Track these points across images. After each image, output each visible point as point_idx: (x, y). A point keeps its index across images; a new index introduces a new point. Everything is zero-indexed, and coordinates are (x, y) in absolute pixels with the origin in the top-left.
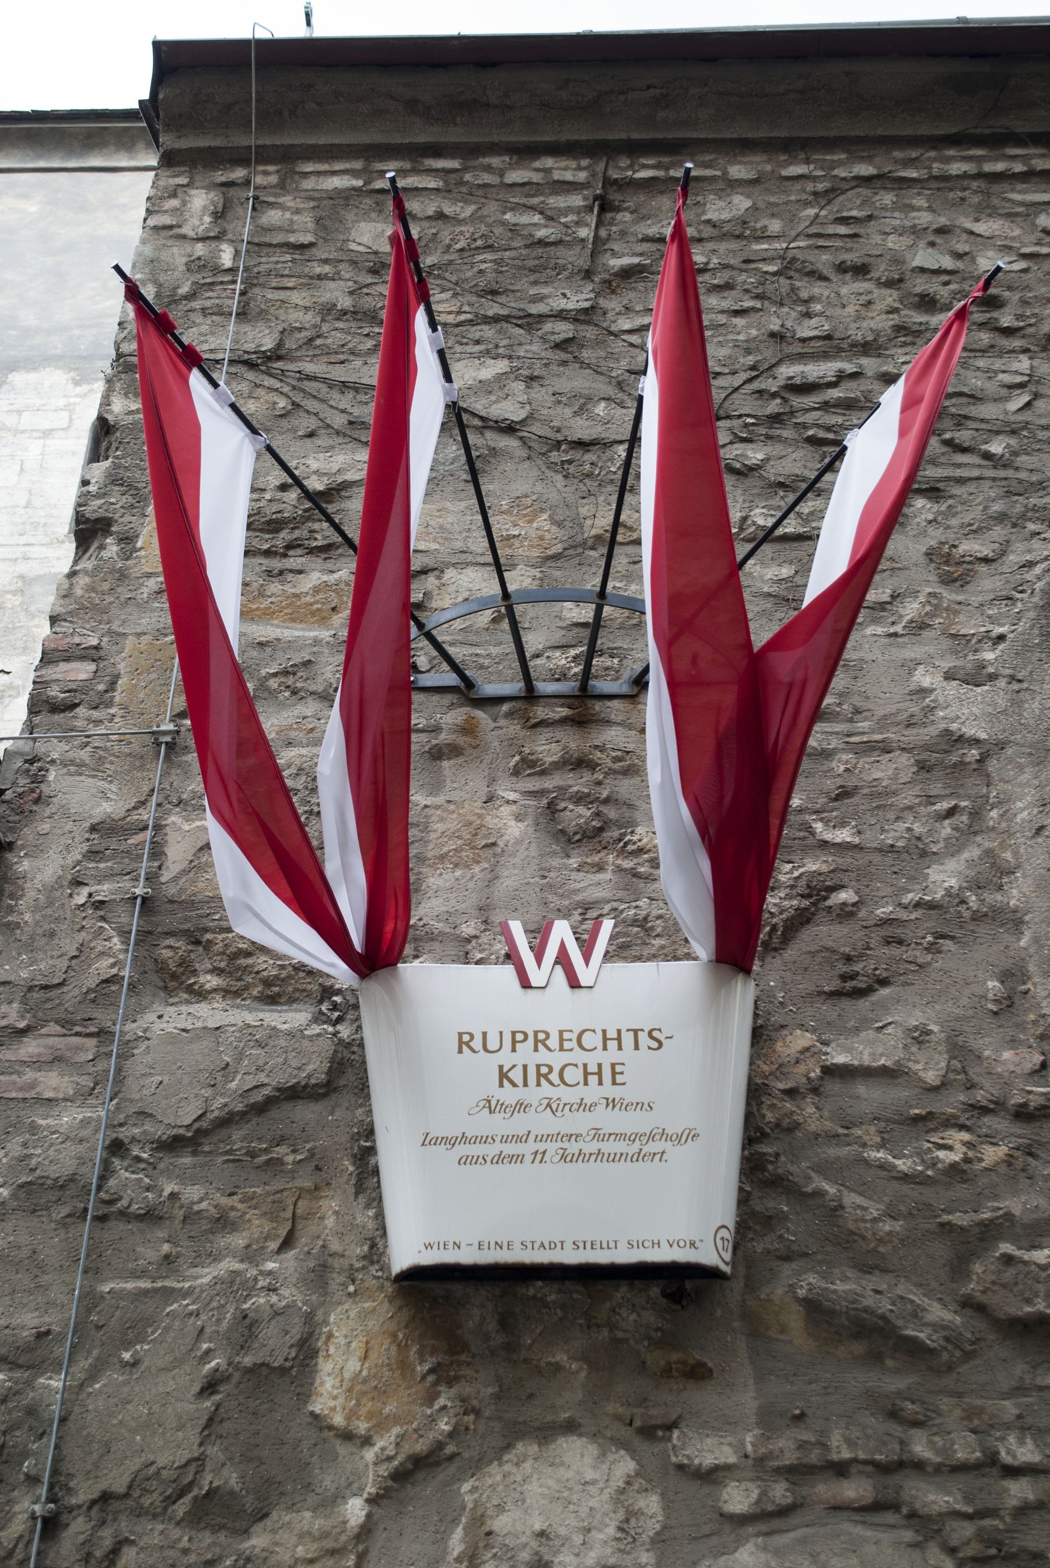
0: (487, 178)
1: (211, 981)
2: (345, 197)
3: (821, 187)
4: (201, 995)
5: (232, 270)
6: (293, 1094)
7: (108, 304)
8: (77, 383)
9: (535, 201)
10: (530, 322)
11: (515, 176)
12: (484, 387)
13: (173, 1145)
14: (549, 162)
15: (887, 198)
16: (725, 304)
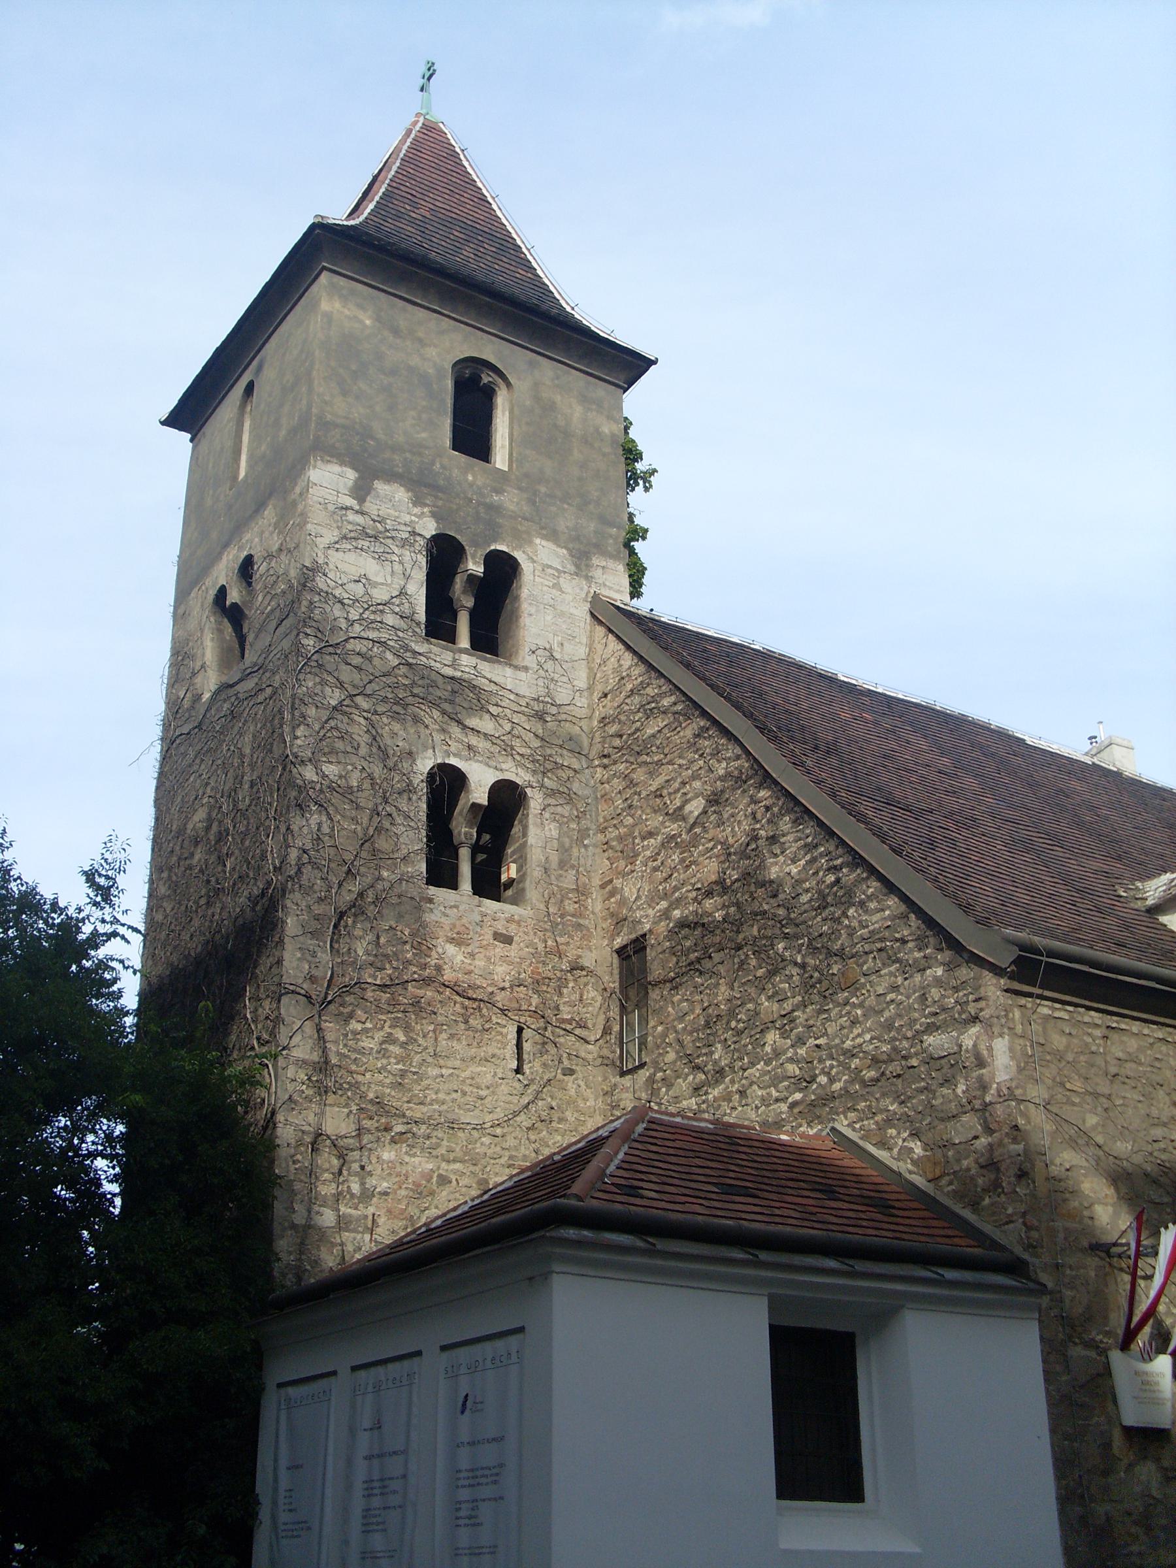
0: (1079, 1018)
1: (1077, 1340)
2: (1047, 1018)
3: (1152, 1040)
4: (1076, 1344)
5: (1033, 1055)
6: (1098, 1375)
7: (424, 435)
8: (415, 504)
9: (1090, 1030)
10: (1096, 1095)
11: (1087, 1019)
12: (1094, 1128)
13: (1082, 1387)
14: (1092, 1013)
15: (1164, 1048)
16: (1136, 1097)
